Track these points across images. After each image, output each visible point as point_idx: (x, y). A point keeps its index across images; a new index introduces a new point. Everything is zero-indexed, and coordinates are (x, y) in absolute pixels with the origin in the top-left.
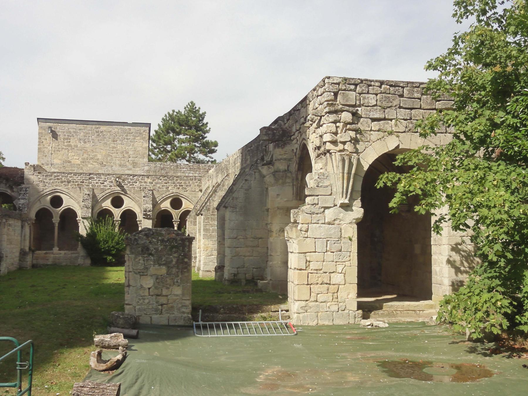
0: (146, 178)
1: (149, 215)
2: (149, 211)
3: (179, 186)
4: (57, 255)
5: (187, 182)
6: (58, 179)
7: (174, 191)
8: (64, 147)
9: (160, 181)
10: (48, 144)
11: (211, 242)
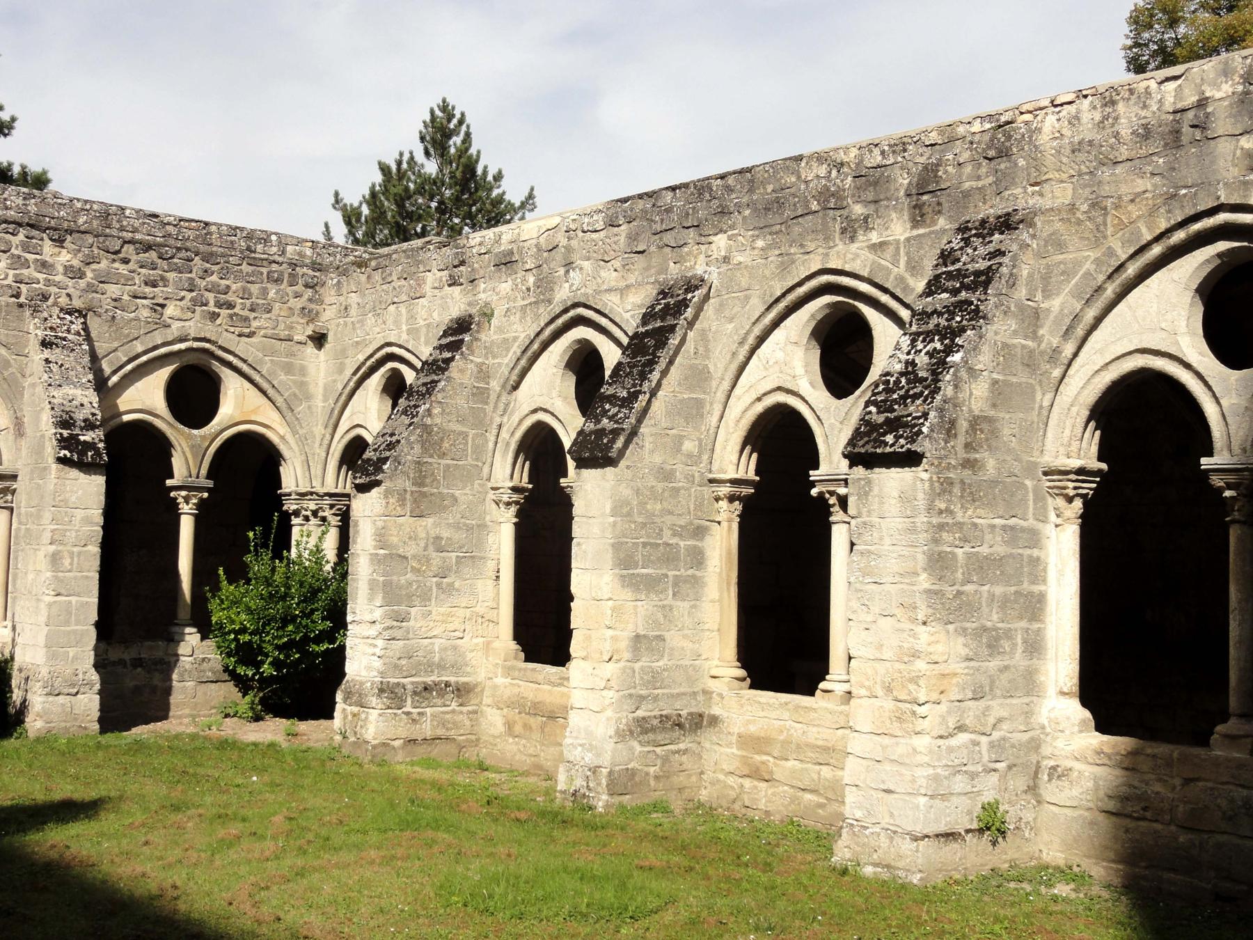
0: (48, 243)
1: (90, 446)
2: (89, 425)
3: (219, 305)
5: (254, 289)
7: (195, 326)
9: (123, 269)
11: (959, 647)
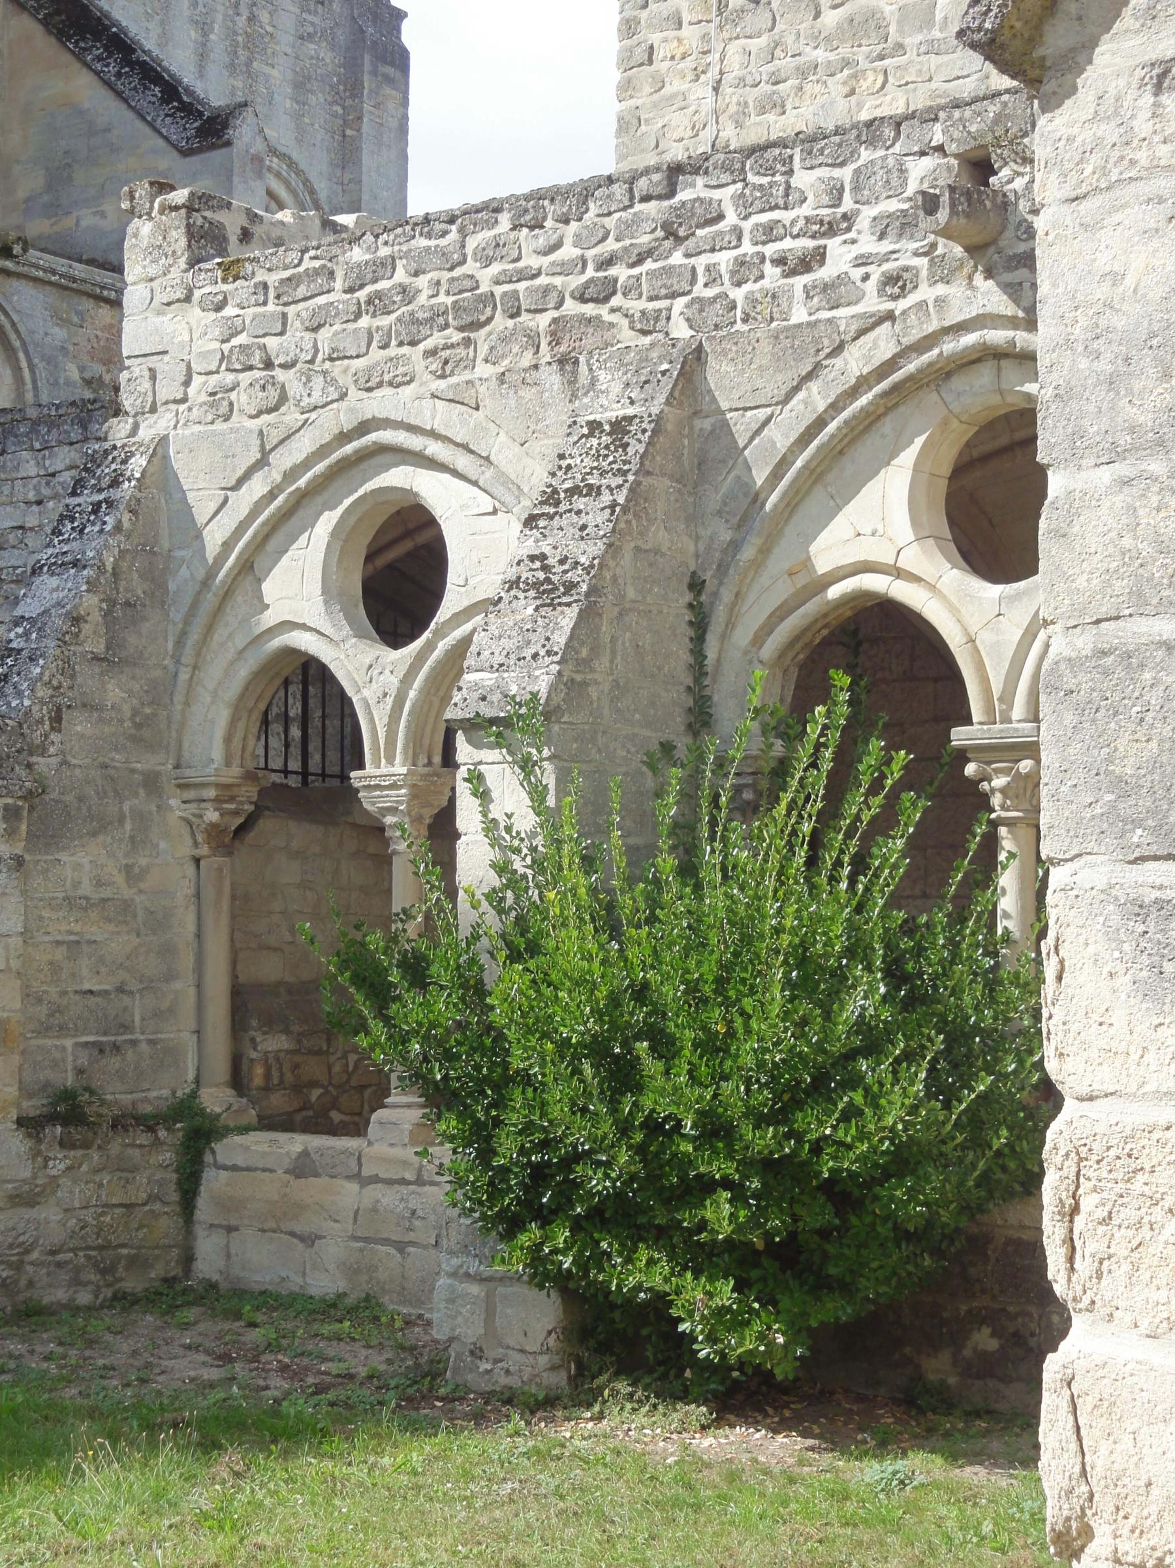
4: (389, 1198)
6: (378, 304)
8: (820, 55)
10: (689, 63)
